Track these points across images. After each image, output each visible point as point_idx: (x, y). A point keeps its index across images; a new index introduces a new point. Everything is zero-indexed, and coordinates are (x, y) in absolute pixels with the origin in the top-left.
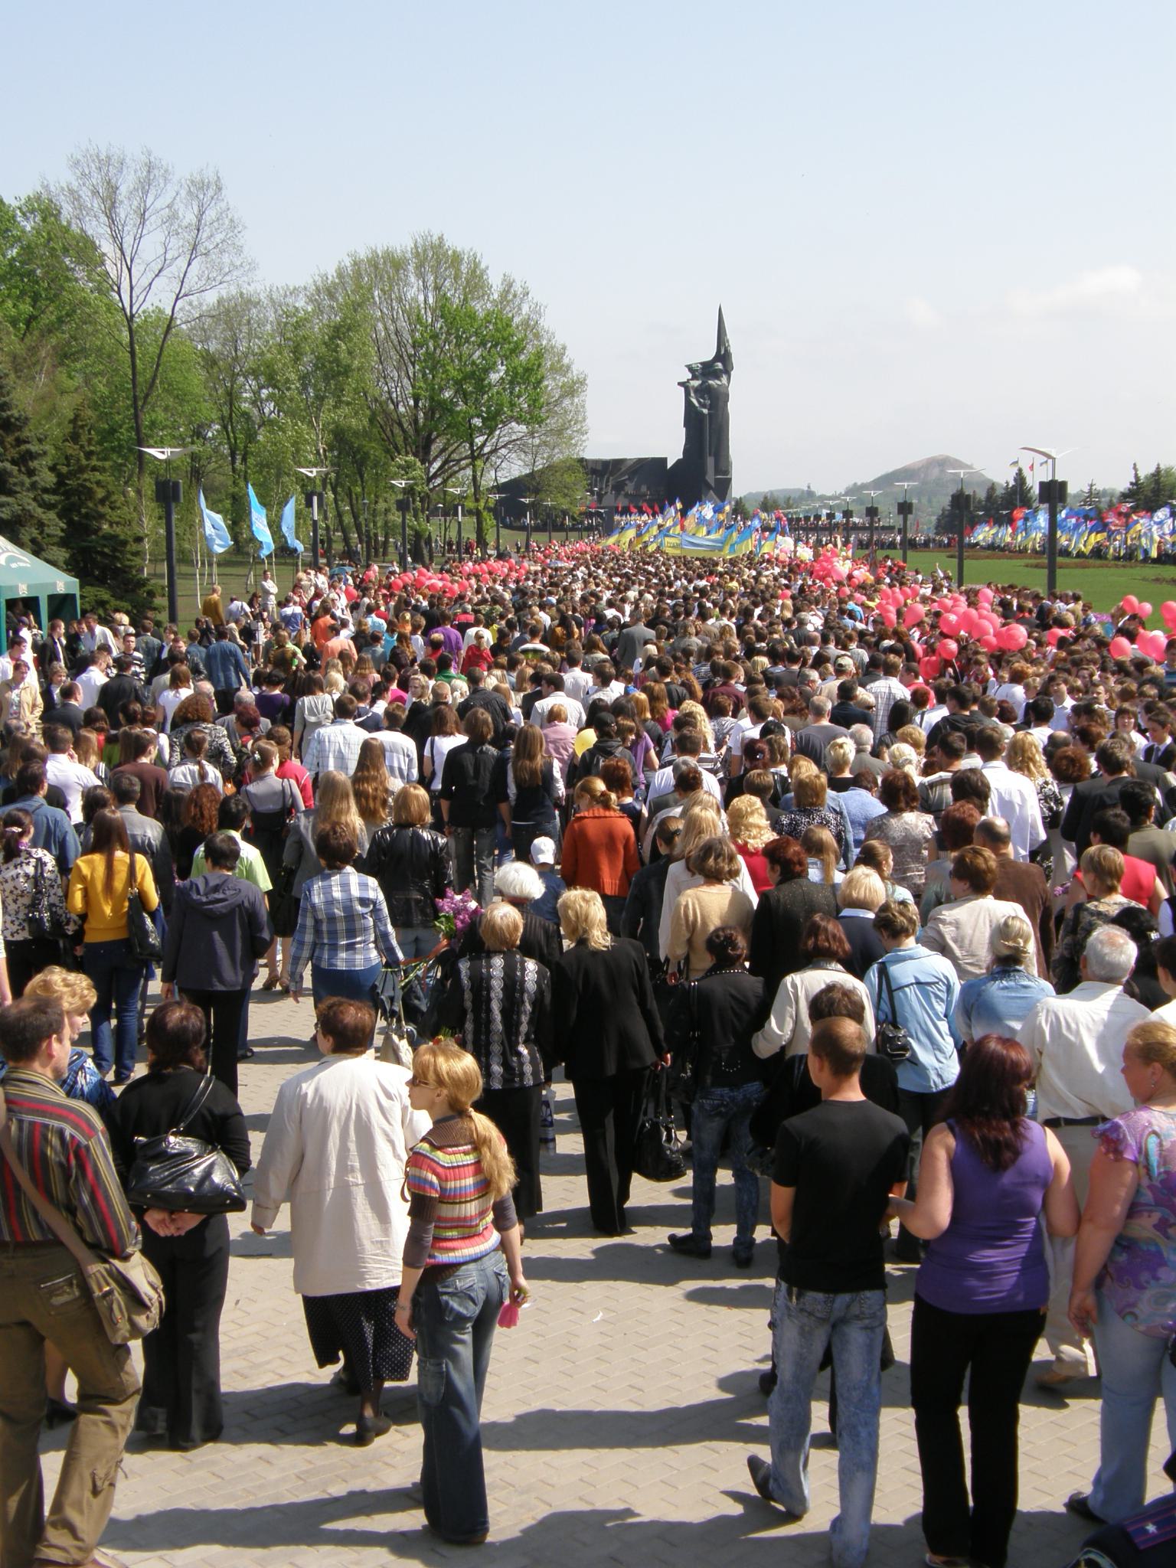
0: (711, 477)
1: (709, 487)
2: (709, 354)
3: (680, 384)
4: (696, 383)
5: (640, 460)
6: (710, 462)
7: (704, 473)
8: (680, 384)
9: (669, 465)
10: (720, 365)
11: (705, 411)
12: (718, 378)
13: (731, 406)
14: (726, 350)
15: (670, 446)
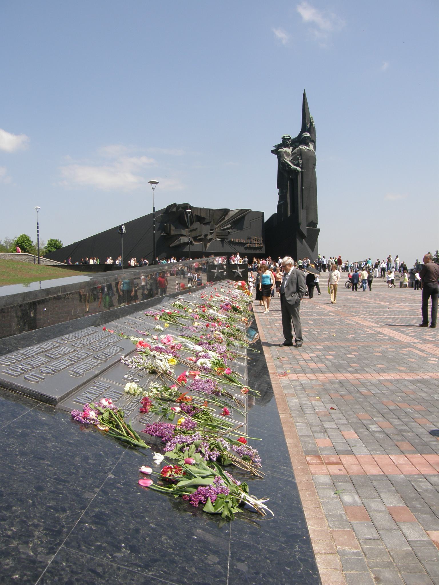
0: (304, 228)
1: (302, 236)
2: (294, 132)
3: (273, 152)
4: (289, 150)
5: (241, 210)
6: (302, 214)
7: (298, 224)
8: (273, 152)
9: (266, 219)
10: (308, 134)
11: (299, 169)
12: (307, 145)
13: (319, 170)
14: (311, 124)
15: (266, 202)
